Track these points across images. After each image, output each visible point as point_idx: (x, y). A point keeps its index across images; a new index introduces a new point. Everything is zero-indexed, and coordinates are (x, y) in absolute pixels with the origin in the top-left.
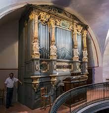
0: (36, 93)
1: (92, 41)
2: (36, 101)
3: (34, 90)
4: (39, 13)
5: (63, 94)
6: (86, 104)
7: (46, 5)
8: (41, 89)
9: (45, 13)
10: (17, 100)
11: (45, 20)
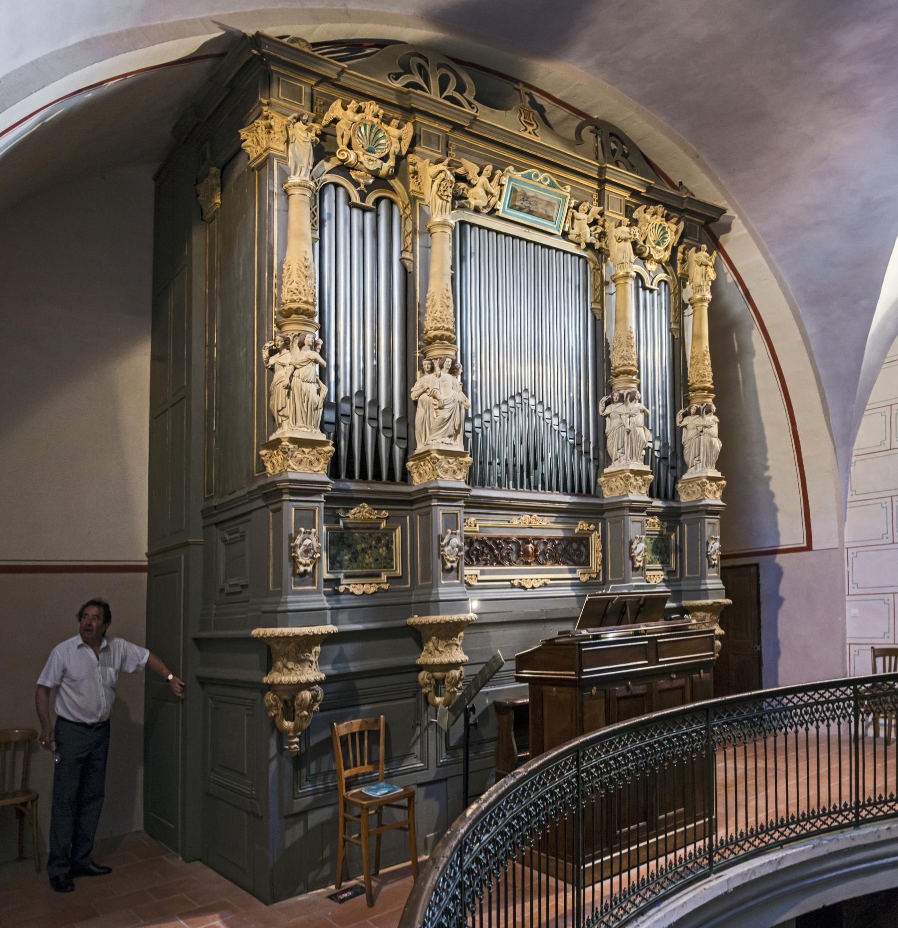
0: (299, 761)
1: (756, 337)
2: (298, 831)
3: (282, 736)
4: (318, 106)
5: (521, 771)
6: (710, 851)
7: (381, 44)
8: (342, 729)
9: (371, 107)
10: (139, 822)
11: (371, 162)
